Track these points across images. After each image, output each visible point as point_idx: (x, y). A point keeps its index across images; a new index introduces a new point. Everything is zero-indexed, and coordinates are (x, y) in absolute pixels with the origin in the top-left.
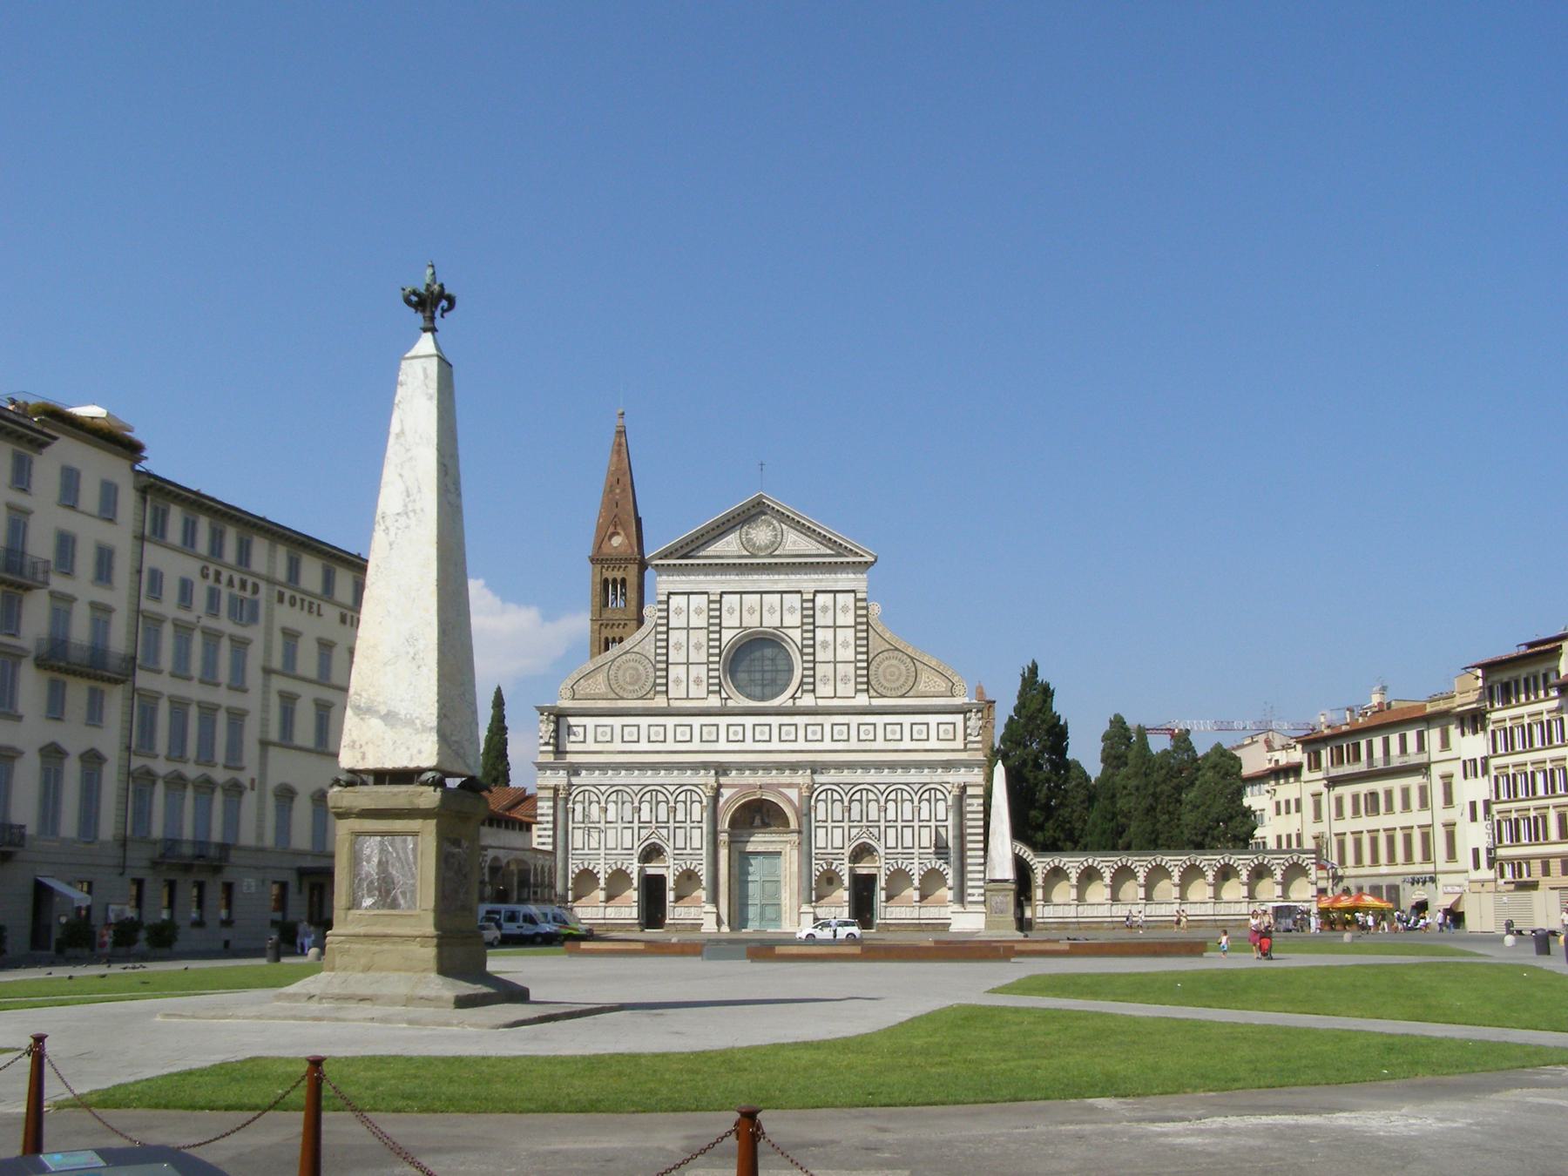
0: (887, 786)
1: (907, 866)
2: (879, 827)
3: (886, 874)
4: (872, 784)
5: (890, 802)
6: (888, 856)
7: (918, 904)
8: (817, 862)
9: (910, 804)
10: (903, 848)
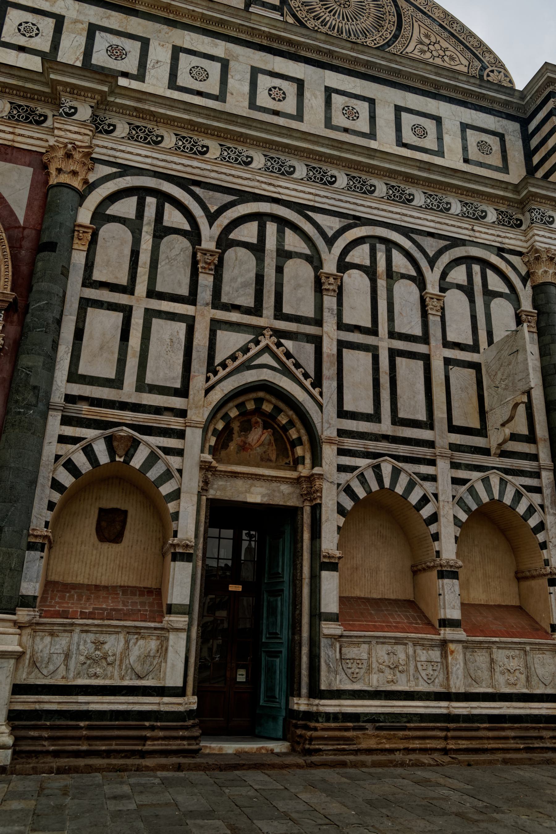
0: (346, 222)
1: (411, 485)
2: (317, 341)
3: (341, 510)
4: (300, 208)
5: (355, 272)
6: (350, 443)
7: (460, 634)
8: (69, 431)
9: (414, 289)
10: (396, 421)
